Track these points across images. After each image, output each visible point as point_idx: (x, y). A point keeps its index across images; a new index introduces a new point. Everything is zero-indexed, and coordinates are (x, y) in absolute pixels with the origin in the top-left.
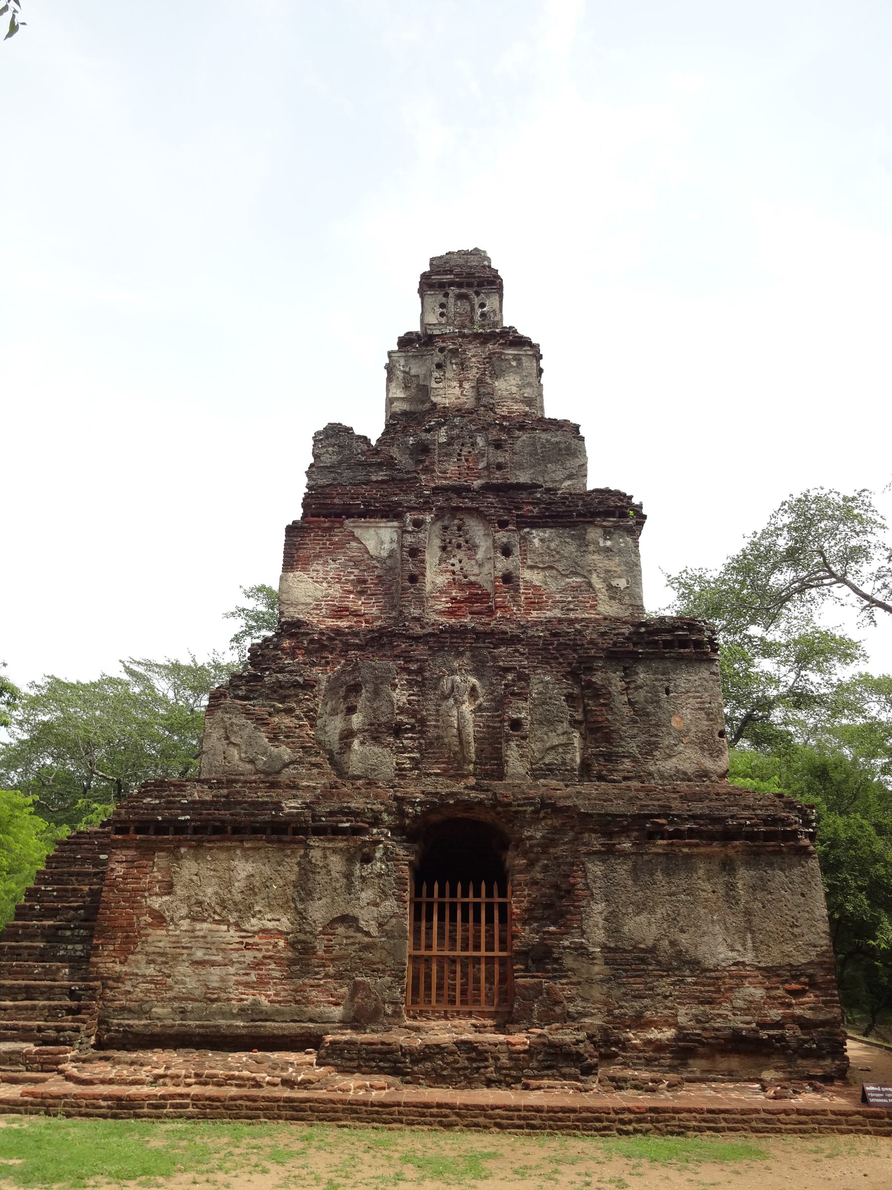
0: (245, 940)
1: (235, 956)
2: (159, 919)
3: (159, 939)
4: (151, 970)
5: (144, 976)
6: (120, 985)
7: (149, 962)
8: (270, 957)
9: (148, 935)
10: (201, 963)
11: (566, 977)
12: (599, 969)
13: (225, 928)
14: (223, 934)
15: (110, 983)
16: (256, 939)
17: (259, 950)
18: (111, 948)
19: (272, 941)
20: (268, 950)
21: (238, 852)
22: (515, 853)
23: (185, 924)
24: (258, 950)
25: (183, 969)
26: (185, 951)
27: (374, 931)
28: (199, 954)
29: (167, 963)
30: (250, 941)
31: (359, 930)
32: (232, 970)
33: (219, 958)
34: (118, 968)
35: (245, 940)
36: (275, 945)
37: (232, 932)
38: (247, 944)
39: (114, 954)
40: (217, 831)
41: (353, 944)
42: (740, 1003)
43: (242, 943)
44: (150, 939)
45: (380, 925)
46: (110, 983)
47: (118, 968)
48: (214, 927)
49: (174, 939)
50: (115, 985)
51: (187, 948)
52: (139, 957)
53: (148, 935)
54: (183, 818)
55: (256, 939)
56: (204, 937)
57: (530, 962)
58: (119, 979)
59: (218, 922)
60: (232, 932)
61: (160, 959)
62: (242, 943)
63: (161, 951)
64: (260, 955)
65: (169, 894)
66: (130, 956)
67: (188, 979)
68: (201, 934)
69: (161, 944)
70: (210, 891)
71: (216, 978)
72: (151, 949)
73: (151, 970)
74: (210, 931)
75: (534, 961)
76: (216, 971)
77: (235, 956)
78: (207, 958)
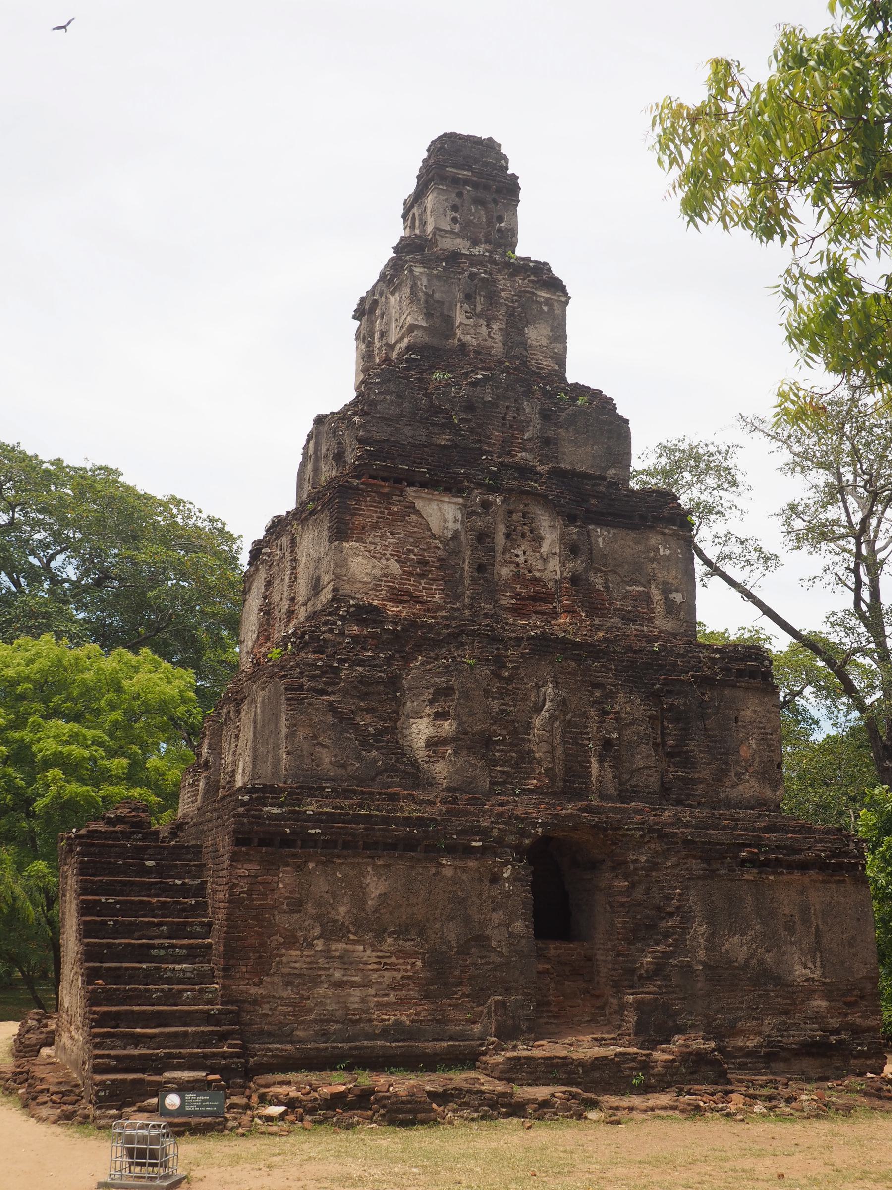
2: (291, 941)
4: (287, 993)
7: (288, 984)
10: (339, 984)
13: (361, 948)
17: (399, 970)
19: (410, 961)
20: (406, 971)
24: (395, 970)
26: (322, 973)
29: (305, 984)
30: (388, 961)
32: (372, 991)
37: (368, 952)
38: (385, 964)
43: (380, 963)
48: (350, 947)
56: (340, 957)
58: (255, 1002)
60: (368, 952)
64: (399, 975)
67: (328, 1001)
68: (338, 954)
69: (297, 965)
71: (357, 999)
73: (287, 993)
74: (346, 951)
78: (345, 979)
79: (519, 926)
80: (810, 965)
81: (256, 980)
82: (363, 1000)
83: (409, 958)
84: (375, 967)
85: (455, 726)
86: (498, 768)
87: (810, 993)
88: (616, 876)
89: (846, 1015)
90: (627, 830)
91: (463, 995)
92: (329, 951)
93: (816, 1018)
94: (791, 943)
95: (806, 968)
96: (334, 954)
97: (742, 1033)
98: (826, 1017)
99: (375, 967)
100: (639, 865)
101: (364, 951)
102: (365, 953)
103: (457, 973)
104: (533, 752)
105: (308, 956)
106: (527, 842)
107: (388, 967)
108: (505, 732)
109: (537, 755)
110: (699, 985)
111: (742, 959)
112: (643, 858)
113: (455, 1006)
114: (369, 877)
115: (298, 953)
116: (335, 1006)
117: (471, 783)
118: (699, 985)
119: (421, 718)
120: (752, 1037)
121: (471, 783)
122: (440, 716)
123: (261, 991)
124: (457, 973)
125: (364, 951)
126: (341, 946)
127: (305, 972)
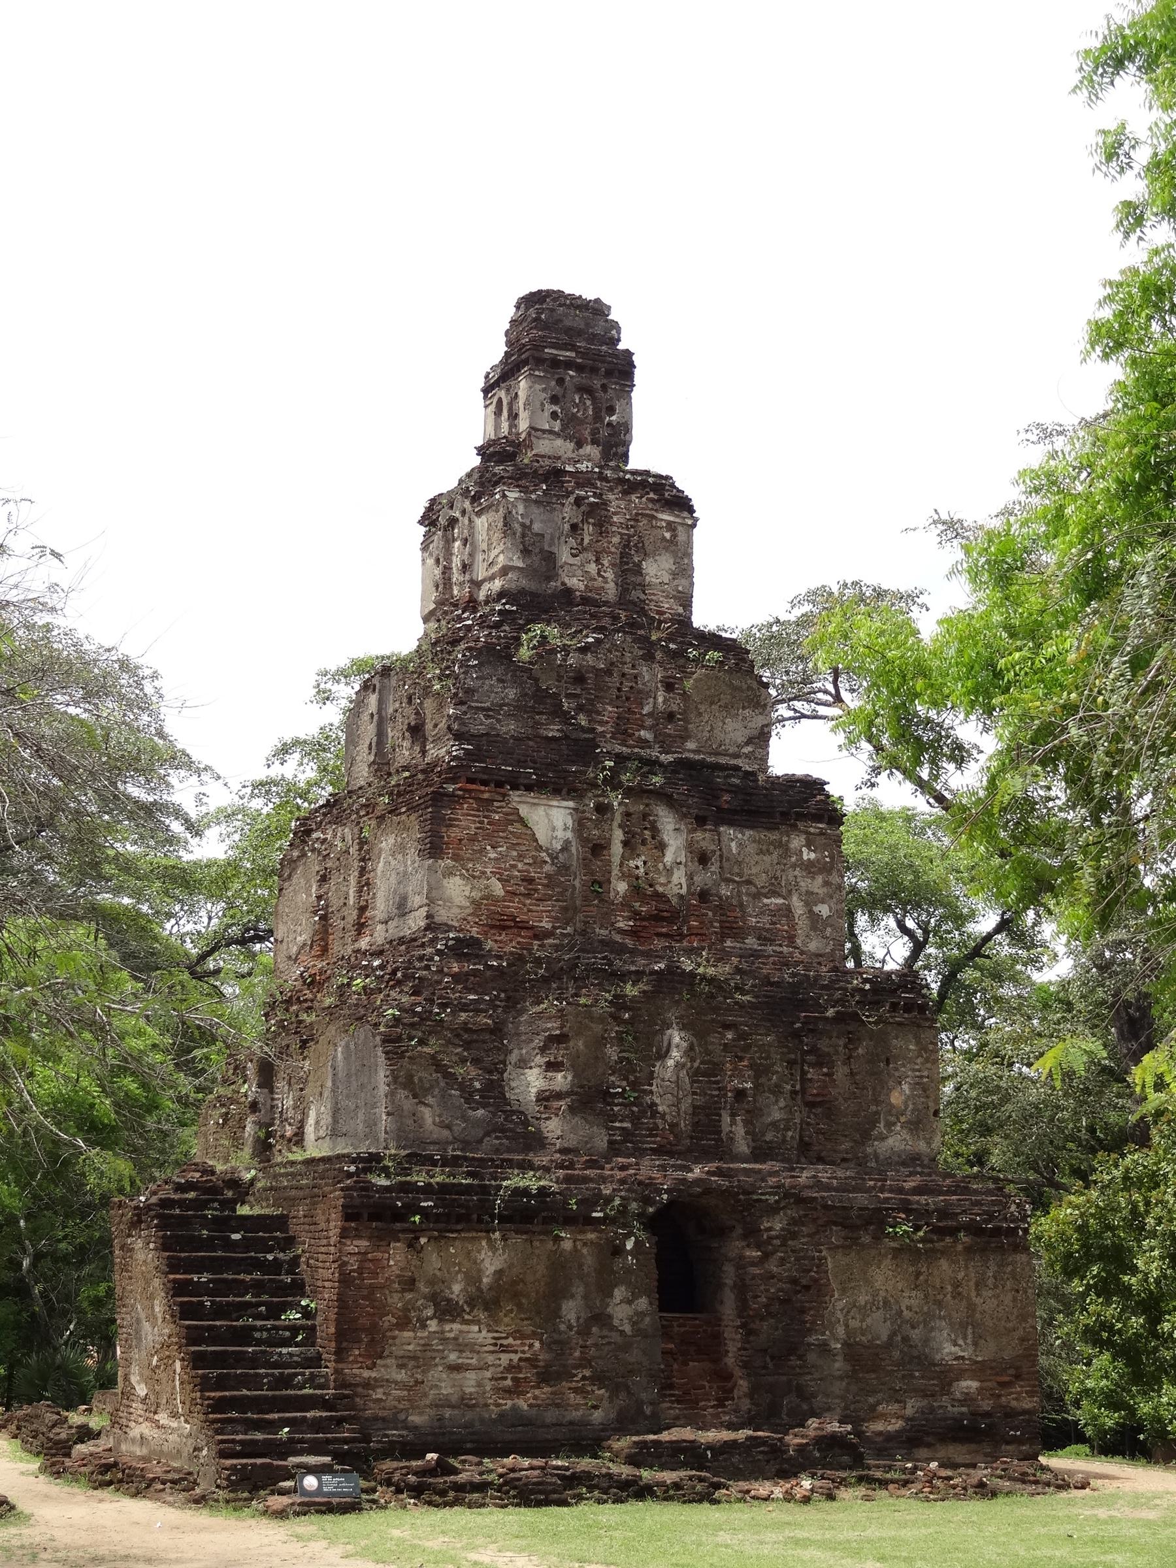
0: (499, 1342)
1: (490, 1359)
2: (404, 1323)
3: (408, 1341)
4: (401, 1376)
5: (396, 1383)
6: (371, 1392)
7: (401, 1366)
8: (527, 1360)
9: (394, 1338)
10: (456, 1368)
11: (809, 1373)
12: (839, 1365)
13: (476, 1328)
14: (476, 1336)
15: (360, 1390)
16: (510, 1341)
17: (516, 1352)
18: (357, 1352)
19: (527, 1342)
20: (523, 1352)
21: (484, 1243)
22: (744, 1244)
23: (433, 1325)
24: (512, 1352)
25: (438, 1374)
26: (436, 1354)
27: (627, 1328)
28: (453, 1357)
29: (419, 1367)
30: (505, 1342)
31: (613, 1328)
32: (488, 1374)
33: (474, 1361)
34: (366, 1374)
35: (499, 1342)
36: (531, 1346)
37: (484, 1332)
38: (502, 1345)
39: (360, 1359)
40: (460, 1219)
41: (609, 1343)
42: (958, 1395)
43: (495, 1345)
44: (397, 1341)
45: (634, 1324)
46: (360, 1390)
47: (366, 1374)
48: (465, 1328)
49: (421, 1342)
50: (365, 1392)
51: (438, 1351)
52: (389, 1361)
53: (394, 1338)
54: (425, 1204)
55: (510, 1341)
56: (455, 1339)
57: (768, 1359)
58: (368, 1384)
59: (467, 1322)
60: (484, 1332)
61: (412, 1363)
62: (495, 1345)
63: (411, 1354)
64: (515, 1357)
65: (411, 1290)
66: (379, 1361)
67: (443, 1385)
68: (452, 1335)
69: (410, 1347)
70: (457, 1288)
71: (473, 1383)
72: (401, 1353)
73: (401, 1376)
74: (461, 1332)
75: (772, 1358)
76: (471, 1376)
77: (490, 1359)
78: (460, 1361)
79: (643, 1303)
80: (961, 1342)
81: (369, 1362)
82: (479, 1384)
83: (526, 1338)
84: (492, 1348)
85: (570, 1078)
86: (617, 1124)
87: (960, 1375)
88: (748, 1246)
89: (999, 1396)
90: (762, 1194)
91: (584, 1378)
92: (443, 1332)
93: (965, 1400)
94: (940, 1318)
95: (955, 1345)
96: (448, 1335)
97: (883, 1416)
98: (976, 1400)
99: (492, 1348)
100: (773, 1233)
101: (480, 1331)
102: (479, 1334)
103: (577, 1354)
104: (656, 1105)
105: (421, 1338)
106: (651, 1210)
107: (505, 1349)
108: (624, 1083)
109: (660, 1109)
110: (837, 1365)
111: (884, 1338)
112: (778, 1226)
113: (576, 1390)
114: (483, 1252)
115: (411, 1334)
116: (450, 1391)
117: (587, 1143)
118: (837, 1365)
119: (531, 1068)
120: (893, 1421)
121: (587, 1143)
122: (552, 1066)
123: (374, 1375)
124: (577, 1354)
125: (480, 1331)
126: (456, 1326)
127: (419, 1354)
